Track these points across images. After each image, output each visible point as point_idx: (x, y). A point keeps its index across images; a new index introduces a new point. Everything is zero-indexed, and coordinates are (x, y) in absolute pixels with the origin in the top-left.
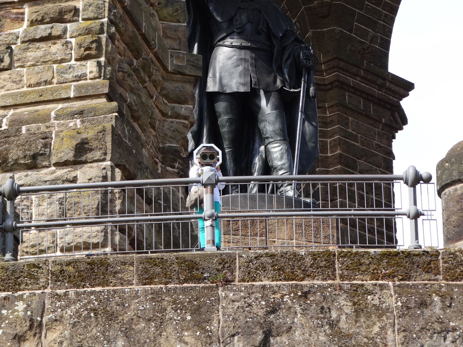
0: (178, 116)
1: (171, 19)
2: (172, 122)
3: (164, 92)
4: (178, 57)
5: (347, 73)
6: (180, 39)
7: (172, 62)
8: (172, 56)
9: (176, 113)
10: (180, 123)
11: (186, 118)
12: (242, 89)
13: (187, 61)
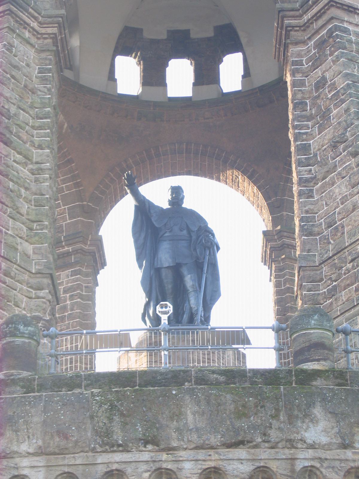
0: (38, 298)
1: (38, 243)
2: (36, 301)
3: (29, 285)
4: (39, 265)
5: (290, 239)
6: (42, 254)
7: (35, 268)
8: (35, 264)
9: (37, 296)
10: (40, 301)
11: (43, 298)
12: (171, 265)
13: (44, 266)
